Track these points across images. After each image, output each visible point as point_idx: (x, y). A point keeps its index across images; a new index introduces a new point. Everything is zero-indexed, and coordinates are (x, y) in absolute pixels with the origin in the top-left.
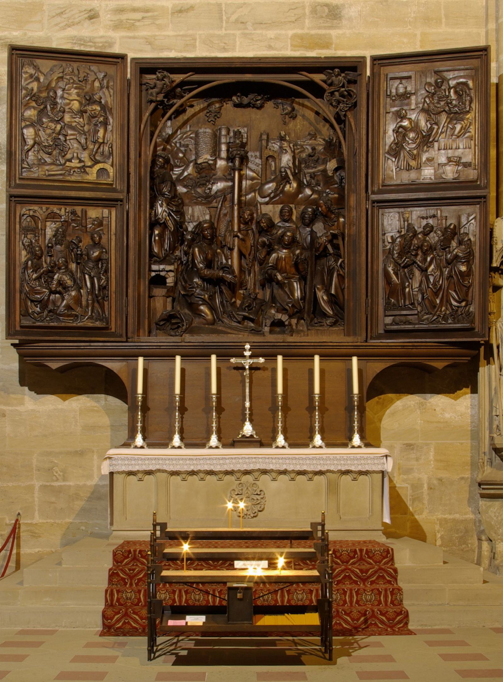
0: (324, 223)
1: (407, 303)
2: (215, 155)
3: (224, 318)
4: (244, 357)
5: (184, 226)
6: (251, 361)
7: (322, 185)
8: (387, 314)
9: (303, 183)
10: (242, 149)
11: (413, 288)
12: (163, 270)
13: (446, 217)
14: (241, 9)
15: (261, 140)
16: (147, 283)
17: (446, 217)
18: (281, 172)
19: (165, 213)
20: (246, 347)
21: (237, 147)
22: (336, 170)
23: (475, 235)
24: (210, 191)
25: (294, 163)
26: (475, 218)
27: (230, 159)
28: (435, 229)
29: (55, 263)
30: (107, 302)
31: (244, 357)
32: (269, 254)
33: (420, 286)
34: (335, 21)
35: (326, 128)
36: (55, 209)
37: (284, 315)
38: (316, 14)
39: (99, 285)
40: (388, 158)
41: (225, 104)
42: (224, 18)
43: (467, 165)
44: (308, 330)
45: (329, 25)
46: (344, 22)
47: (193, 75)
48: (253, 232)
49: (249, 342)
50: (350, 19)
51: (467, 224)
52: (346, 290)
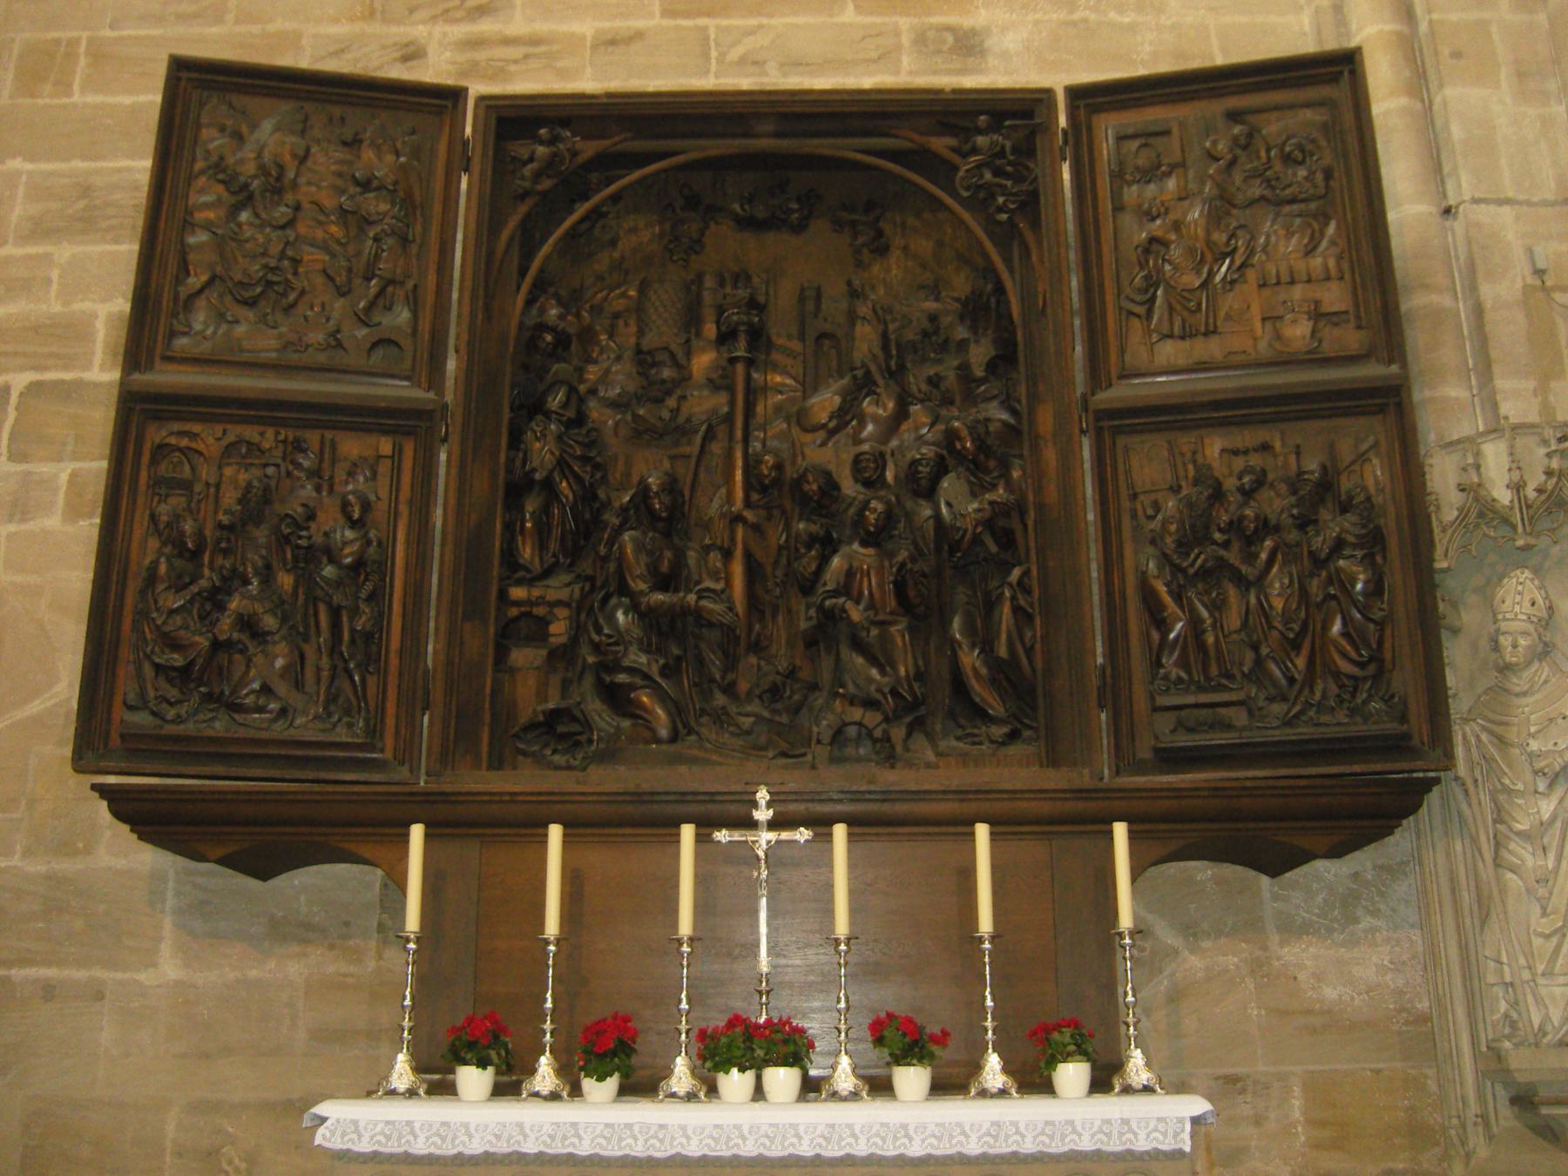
0: (970, 482)
1: (1214, 671)
2: (689, 332)
3: (701, 725)
4: (752, 825)
5: (602, 494)
6: (772, 836)
7: (958, 402)
8: (1163, 701)
9: (911, 395)
10: (754, 312)
11: (1226, 632)
12: (541, 601)
13: (1298, 447)
14: (752, 38)
15: (802, 300)
16: (492, 630)
17: (1298, 447)
18: (853, 369)
19: (548, 456)
20: (759, 795)
21: (739, 307)
22: (992, 366)
23: (1383, 490)
24: (674, 418)
25: (885, 347)
26: (1376, 445)
27: (725, 337)
28: (1271, 476)
29: (234, 570)
30: (375, 677)
31: (752, 825)
32: (824, 560)
33: (1245, 624)
34: (972, 59)
35: (962, 276)
36: (250, 433)
37: (868, 714)
38: (927, 46)
39: (353, 631)
40: (1131, 313)
41: (712, 225)
42: (714, 54)
43: (1335, 318)
44: (939, 754)
45: (959, 66)
46: (992, 61)
47: (626, 140)
48: (784, 512)
49: (766, 784)
50: (1005, 55)
51: (1353, 463)
52: (1038, 646)
